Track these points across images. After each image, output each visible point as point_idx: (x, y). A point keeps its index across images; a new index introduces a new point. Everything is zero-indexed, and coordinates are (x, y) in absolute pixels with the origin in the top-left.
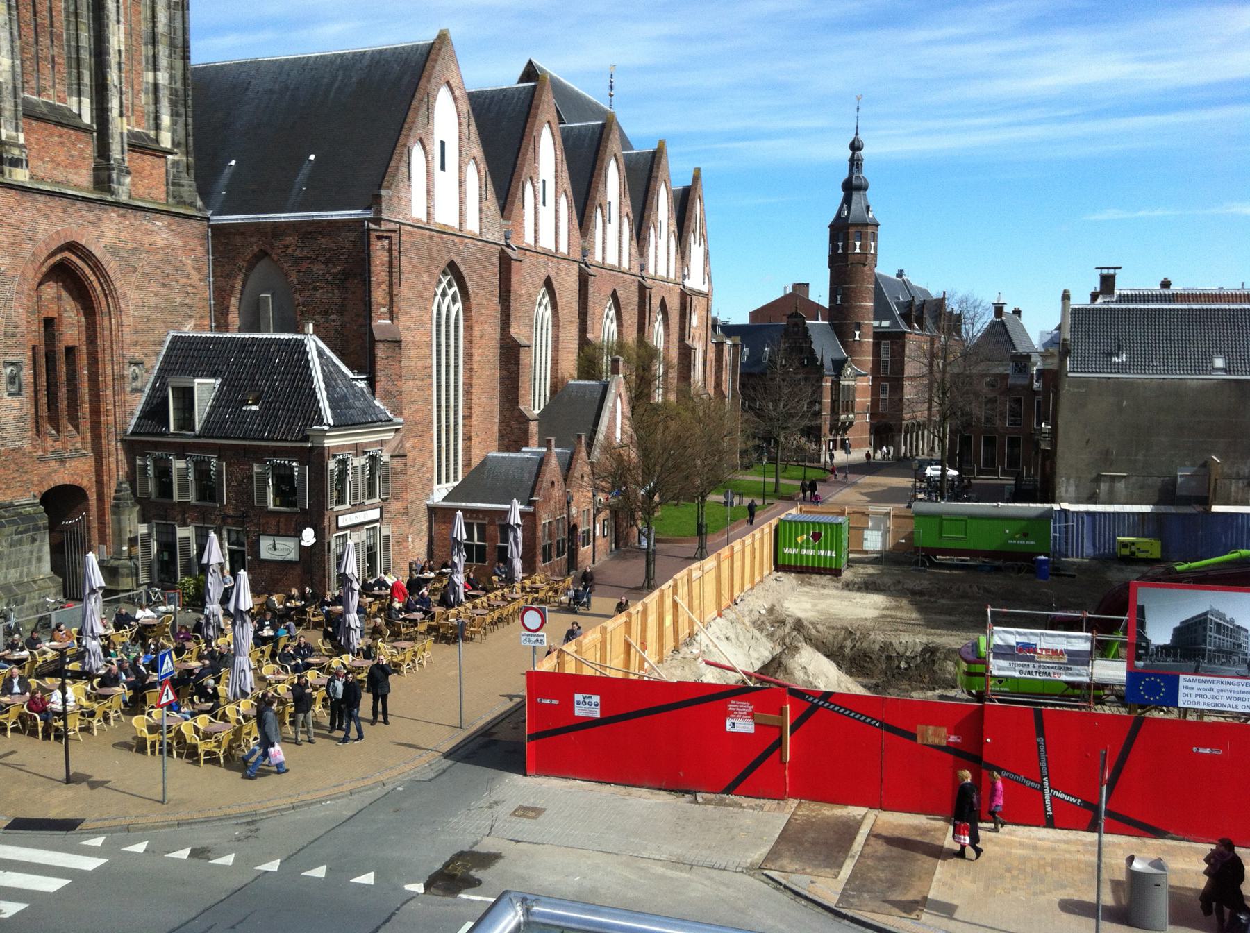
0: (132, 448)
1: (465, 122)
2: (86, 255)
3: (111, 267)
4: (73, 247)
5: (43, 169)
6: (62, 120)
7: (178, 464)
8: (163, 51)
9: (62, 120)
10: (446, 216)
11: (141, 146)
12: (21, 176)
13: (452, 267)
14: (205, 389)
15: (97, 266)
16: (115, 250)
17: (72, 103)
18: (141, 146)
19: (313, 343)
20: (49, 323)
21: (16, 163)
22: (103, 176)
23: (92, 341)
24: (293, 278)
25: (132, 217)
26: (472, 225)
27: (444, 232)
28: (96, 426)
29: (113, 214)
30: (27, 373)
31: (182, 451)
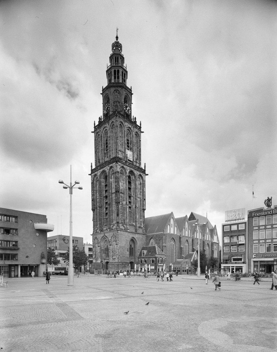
0: (138, 258)
1: (175, 222)
2: (134, 238)
3: (137, 239)
4: (133, 237)
5: (131, 230)
6: (133, 225)
7: (143, 259)
8: (142, 217)
9: (133, 225)
10: (172, 232)
11: (140, 227)
12: (129, 231)
13: (173, 238)
14: (145, 252)
15: (135, 240)
16: (137, 238)
17: (133, 223)
18: (140, 227)
19: (156, 246)
20: (131, 245)
21: (128, 229)
22: (136, 231)
23: (135, 247)
24: (155, 240)
25: (139, 235)
26: (176, 233)
27: (172, 234)
28: (135, 256)
29: (137, 234)
30: (129, 250)
31: (143, 258)
